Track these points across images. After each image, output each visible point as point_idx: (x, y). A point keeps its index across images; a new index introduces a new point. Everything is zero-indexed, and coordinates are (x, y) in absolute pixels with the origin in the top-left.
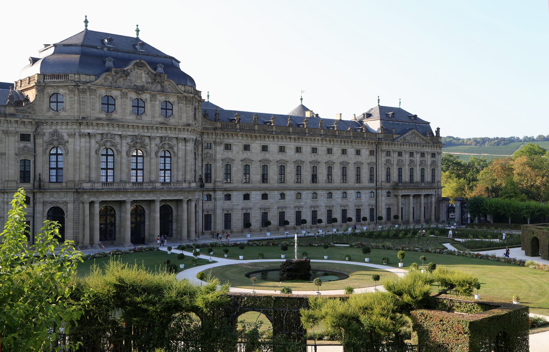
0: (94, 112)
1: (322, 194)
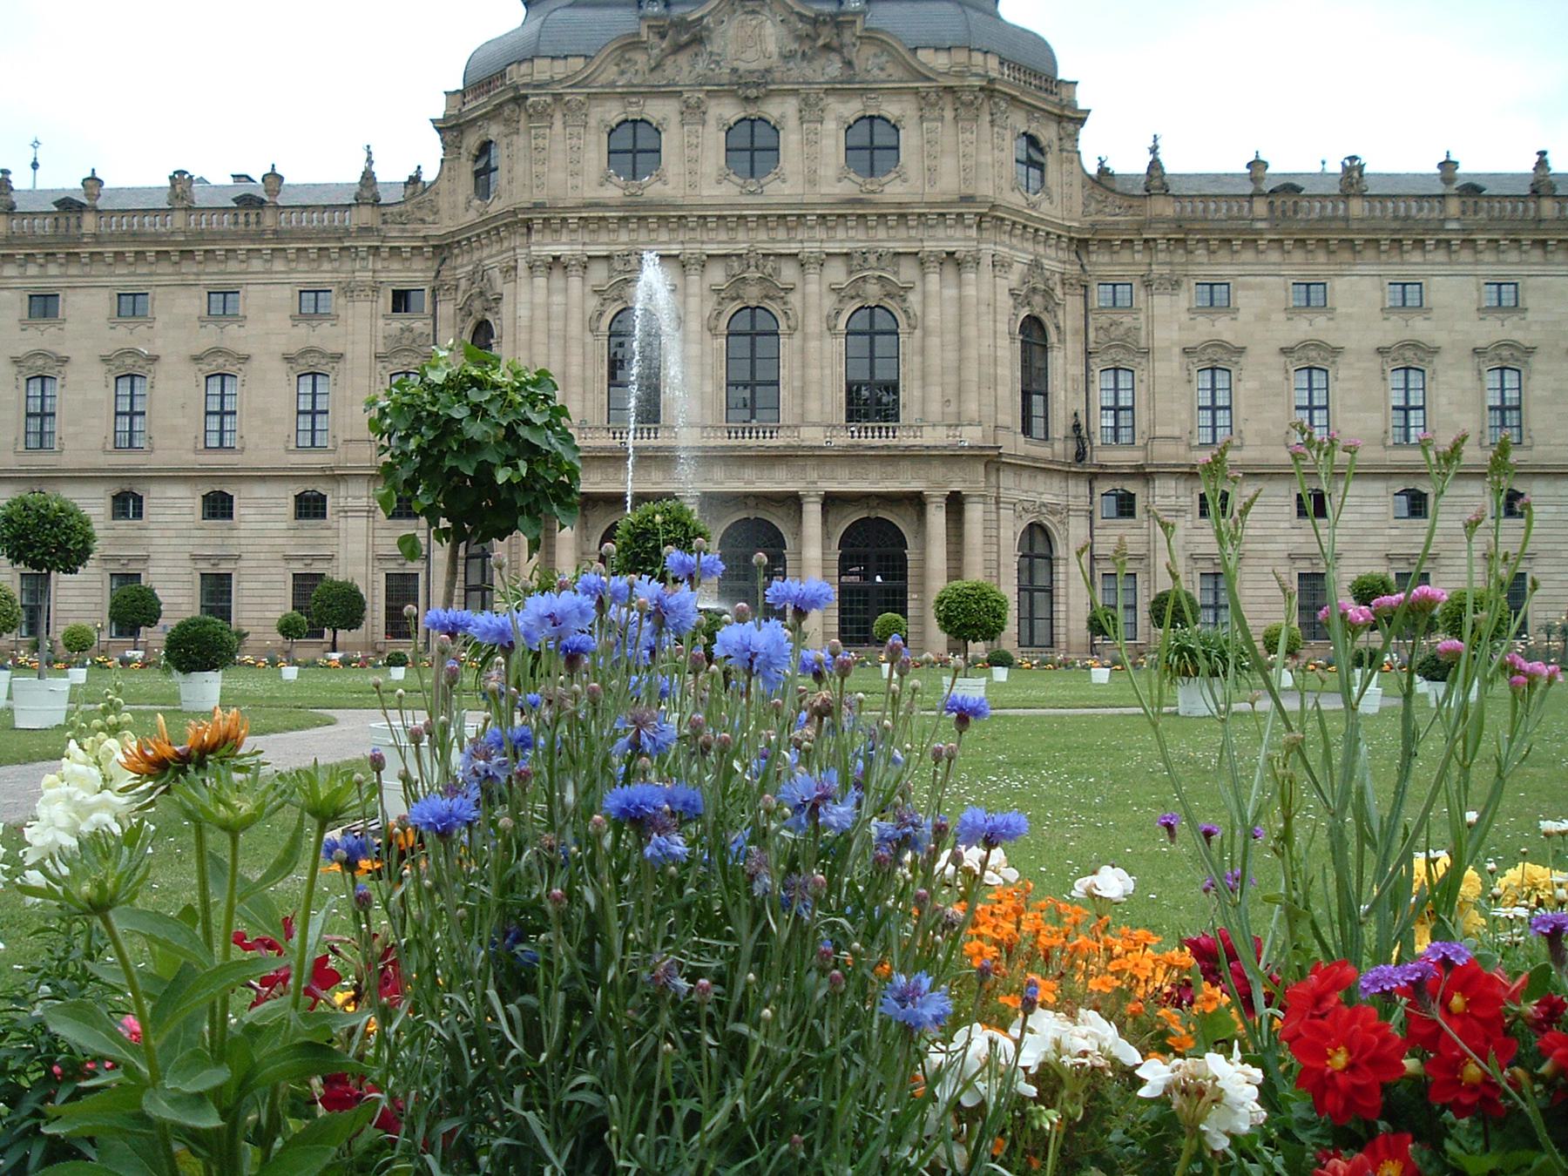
0: (579, 181)
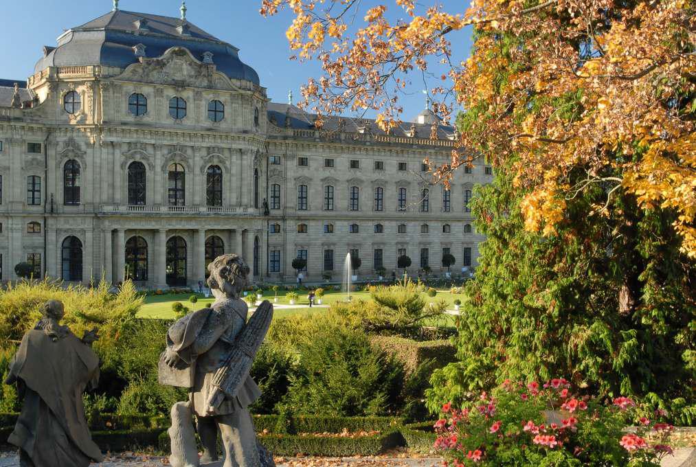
1: (435, 227)
